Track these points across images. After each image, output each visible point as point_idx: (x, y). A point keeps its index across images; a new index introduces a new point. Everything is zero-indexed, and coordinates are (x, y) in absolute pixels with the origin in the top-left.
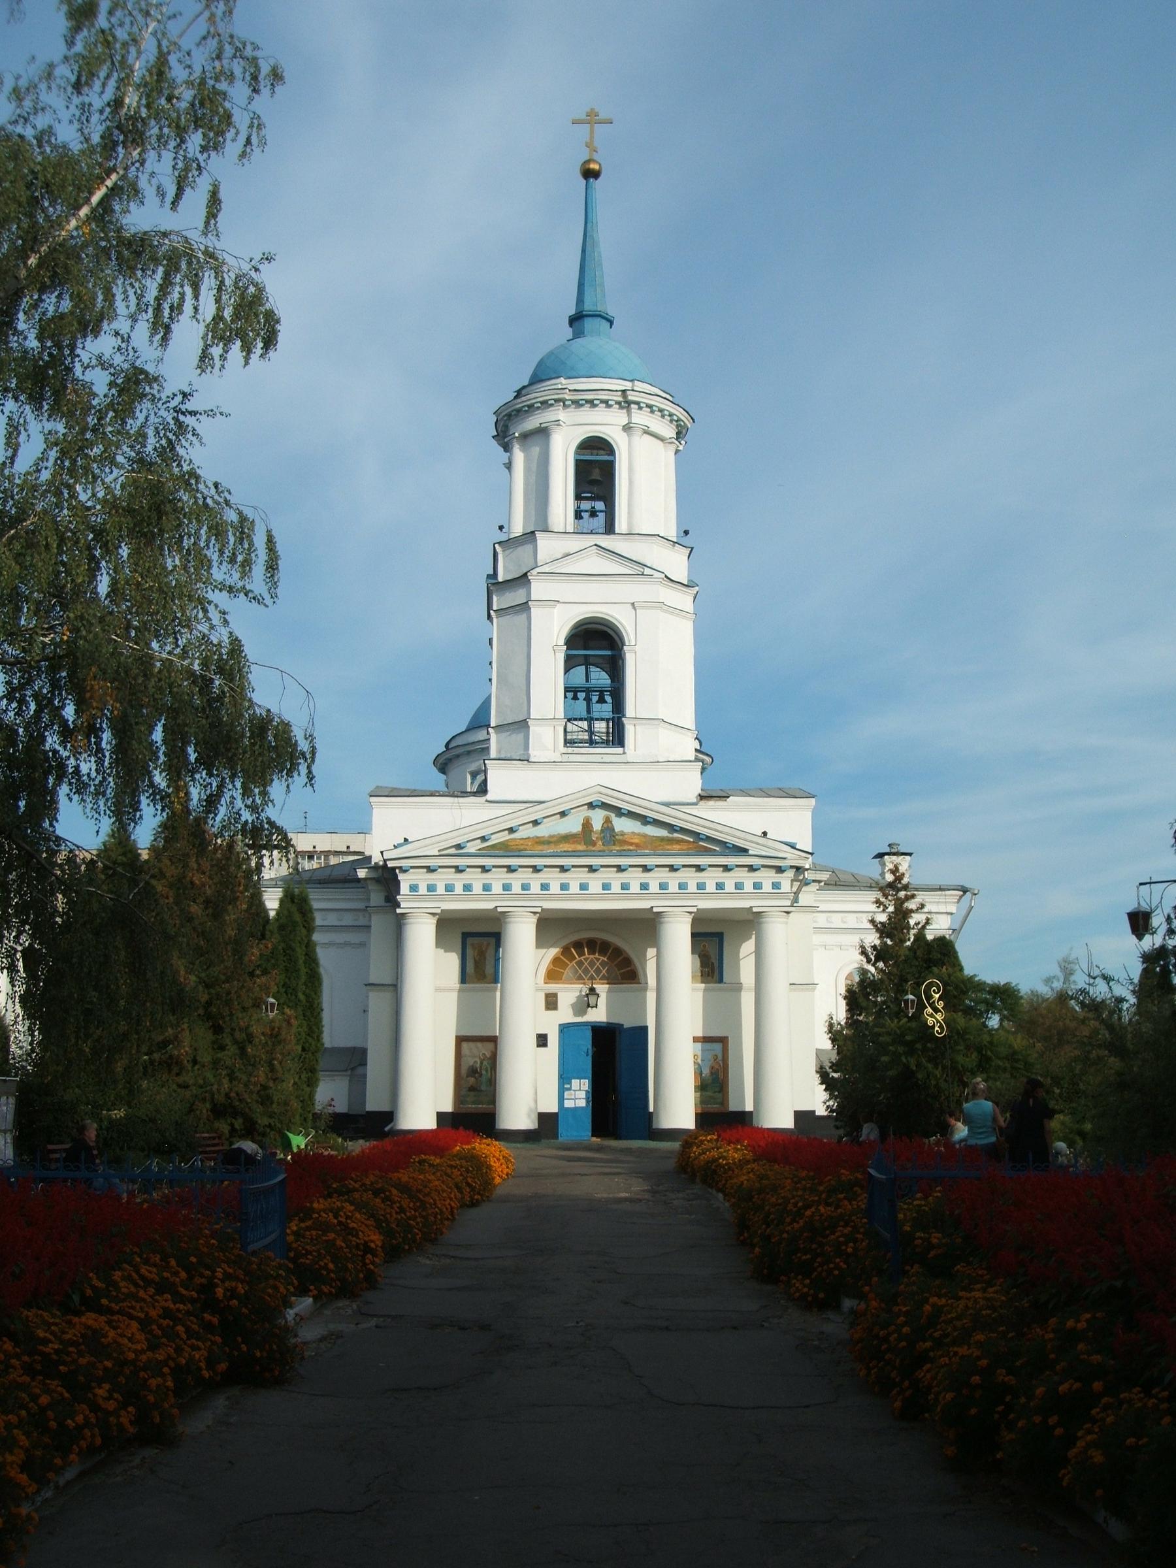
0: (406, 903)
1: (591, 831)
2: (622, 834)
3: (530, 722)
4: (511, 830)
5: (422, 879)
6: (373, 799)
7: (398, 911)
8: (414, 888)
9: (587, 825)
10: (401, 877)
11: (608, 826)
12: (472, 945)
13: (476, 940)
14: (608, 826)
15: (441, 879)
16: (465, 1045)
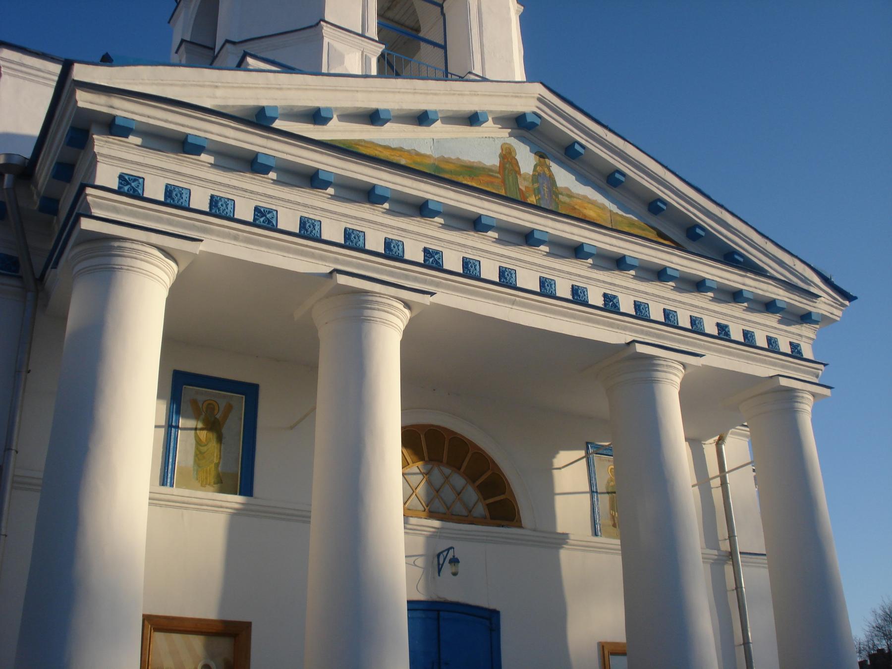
0: (103, 214)
1: (517, 172)
2: (570, 195)
3: (326, 30)
4: (374, 117)
5: (158, 172)
6: (7, 53)
7: (86, 224)
8: (130, 187)
9: (507, 157)
10: (102, 144)
11: (542, 178)
12: (194, 402)
13: (202, 394)
14: (542, 178)
15: (202, 180)
16: (159, 639)
